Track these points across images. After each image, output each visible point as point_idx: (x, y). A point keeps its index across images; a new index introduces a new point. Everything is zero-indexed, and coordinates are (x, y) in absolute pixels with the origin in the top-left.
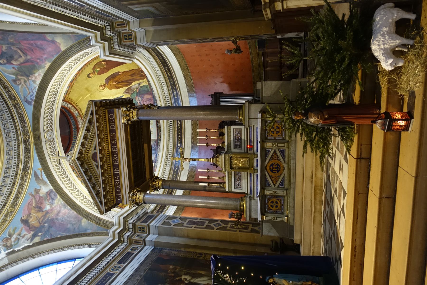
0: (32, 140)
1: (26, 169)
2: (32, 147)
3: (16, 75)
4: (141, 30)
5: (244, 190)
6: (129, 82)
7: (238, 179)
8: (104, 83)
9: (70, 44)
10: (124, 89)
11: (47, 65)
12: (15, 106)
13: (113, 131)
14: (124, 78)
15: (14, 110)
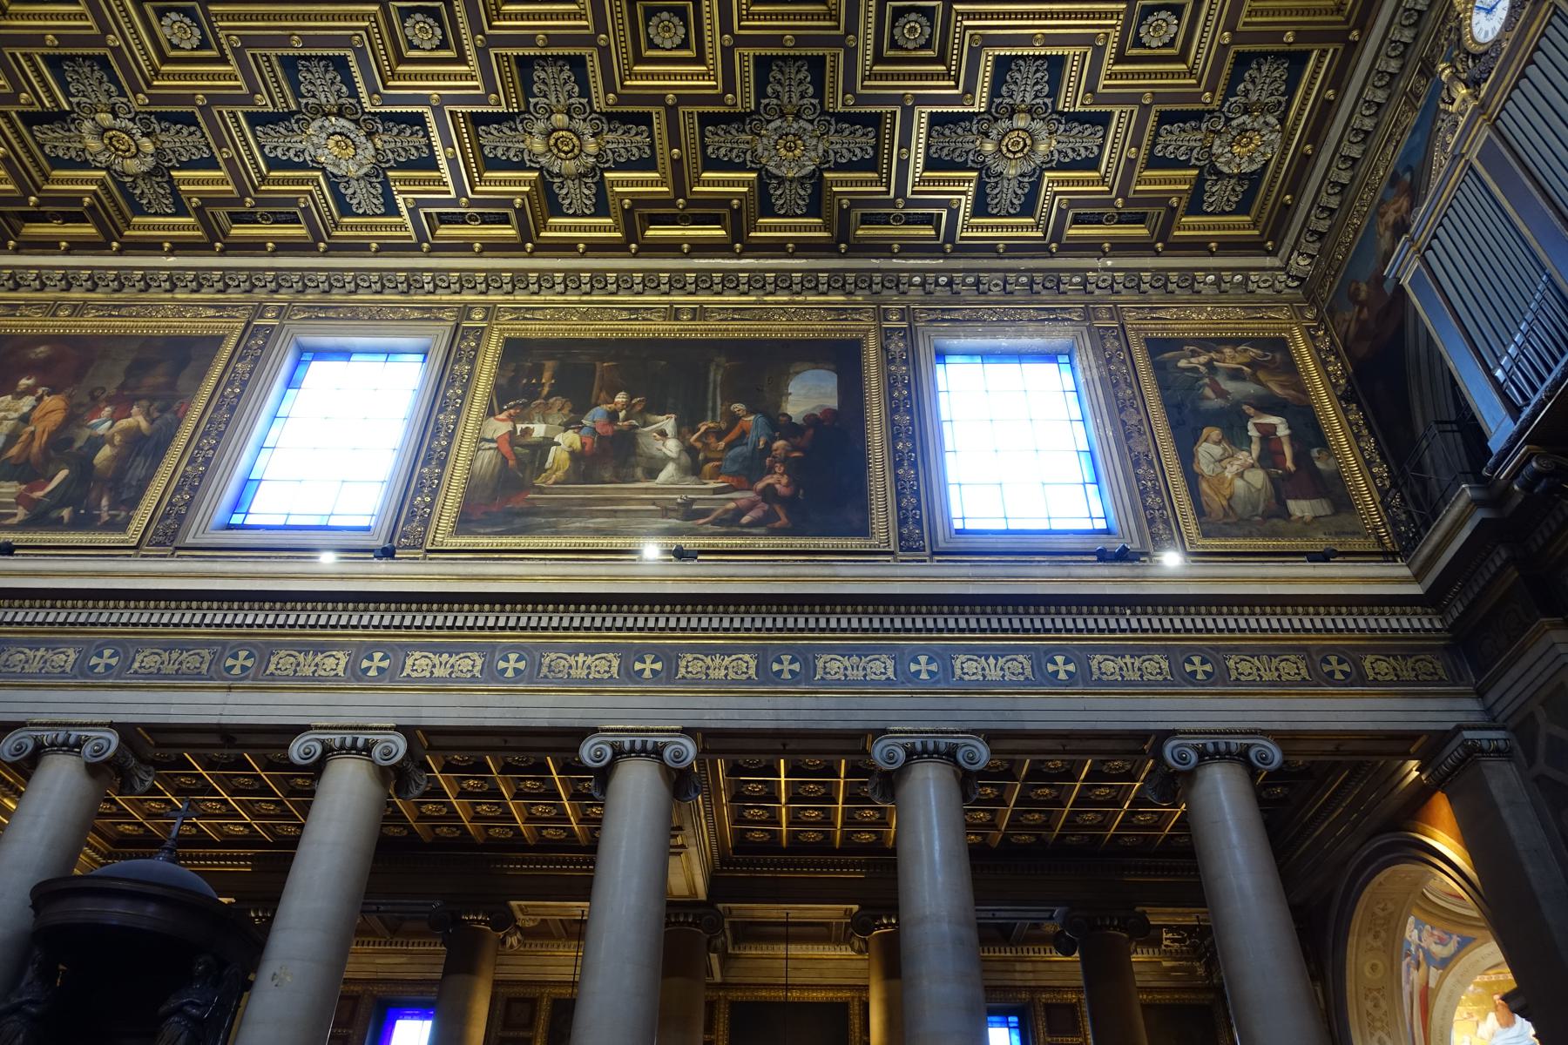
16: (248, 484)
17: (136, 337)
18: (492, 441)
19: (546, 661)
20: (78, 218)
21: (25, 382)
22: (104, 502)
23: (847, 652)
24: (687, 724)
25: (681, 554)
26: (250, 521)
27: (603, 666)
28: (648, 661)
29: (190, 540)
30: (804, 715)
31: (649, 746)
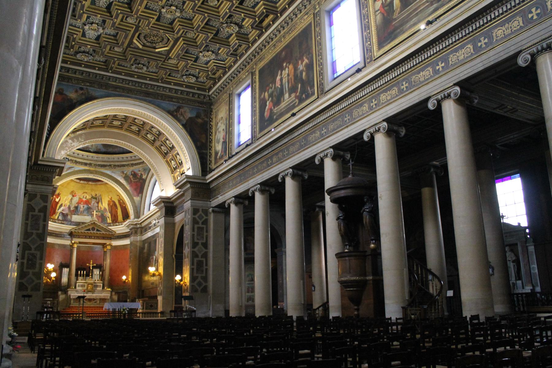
0: (92, 169)
1: (76, 162)
2: (87, 168)
3: (126, 174)
4: (138, 240)
5: (77, 288)
6: (111, 213)
7: (82, 286)
8: (113, 199)
9: (136, 202)
10: (107, 207)
11: (128, 187)
12: (110, 165)
13: (104, 238)
14: (113, 211)
15: (108, 164)
16: (334, 63)
17: (297, 36)
18: (379, 10)
19: (413, 80)
20: (267, 16)
21: (285, 64)
22: (309, 88)
23: (502, 24)
24: (455, 82)
25: (429, 23)
26: (338, 74)
27: (427, 73)
28: (440, 64)
29: (326, 89)
30: (492, 58)
31: (446, 95)
